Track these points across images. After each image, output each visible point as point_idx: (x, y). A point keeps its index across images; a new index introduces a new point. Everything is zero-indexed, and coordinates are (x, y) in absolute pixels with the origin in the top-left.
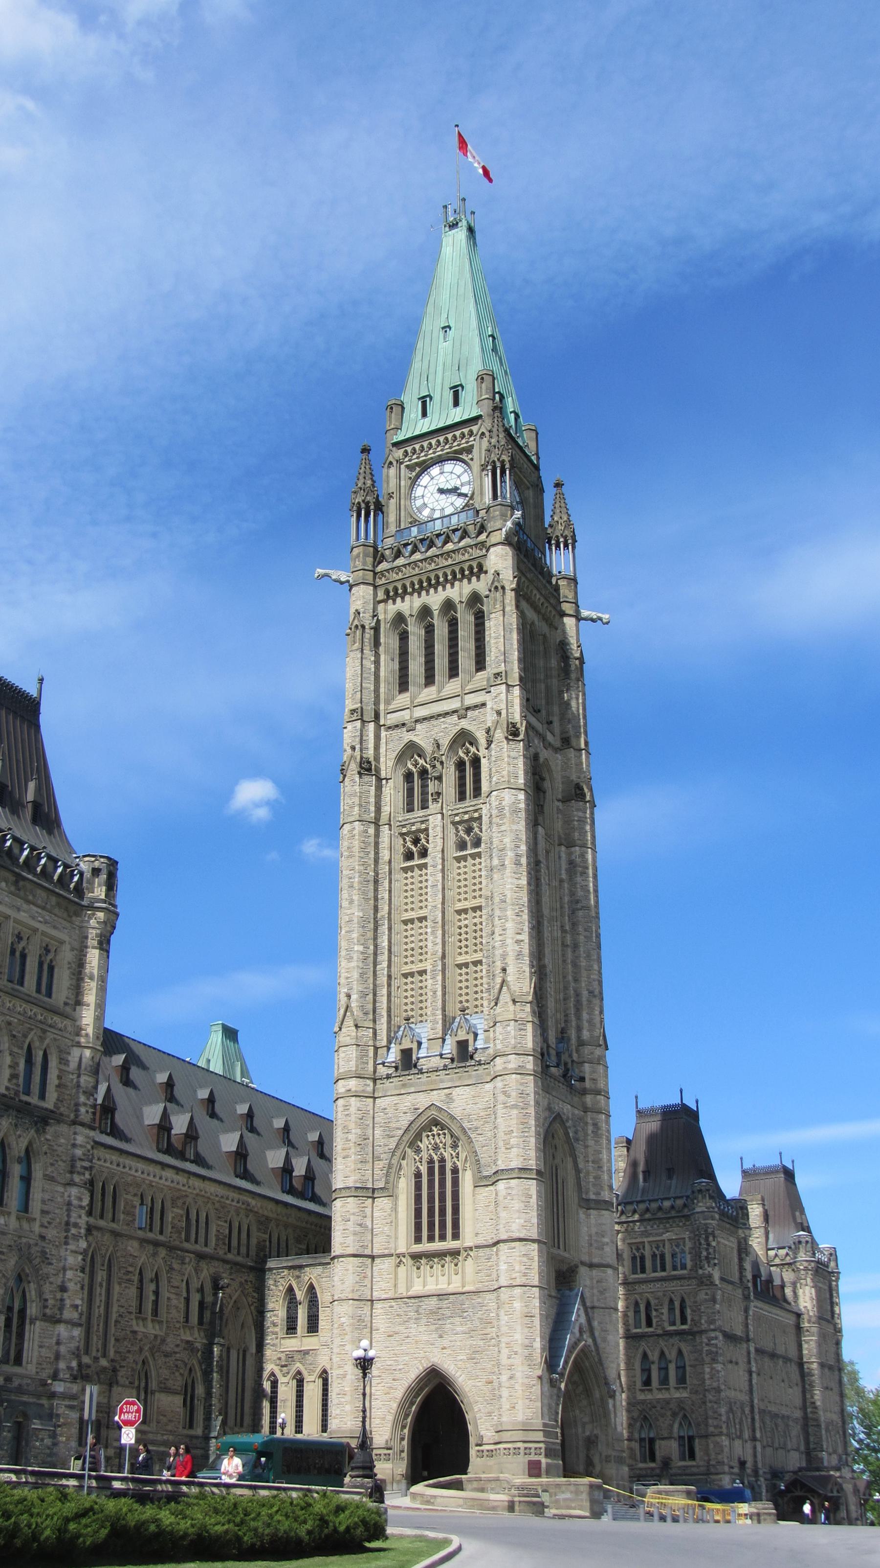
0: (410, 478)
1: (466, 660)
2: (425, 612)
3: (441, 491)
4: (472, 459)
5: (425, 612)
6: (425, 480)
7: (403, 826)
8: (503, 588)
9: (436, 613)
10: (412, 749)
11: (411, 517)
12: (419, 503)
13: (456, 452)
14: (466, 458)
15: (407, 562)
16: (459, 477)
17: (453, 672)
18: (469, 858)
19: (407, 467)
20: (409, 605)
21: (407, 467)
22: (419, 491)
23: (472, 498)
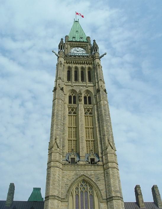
7: (69, 106)
10: (73, 91)
17: (83, 80)
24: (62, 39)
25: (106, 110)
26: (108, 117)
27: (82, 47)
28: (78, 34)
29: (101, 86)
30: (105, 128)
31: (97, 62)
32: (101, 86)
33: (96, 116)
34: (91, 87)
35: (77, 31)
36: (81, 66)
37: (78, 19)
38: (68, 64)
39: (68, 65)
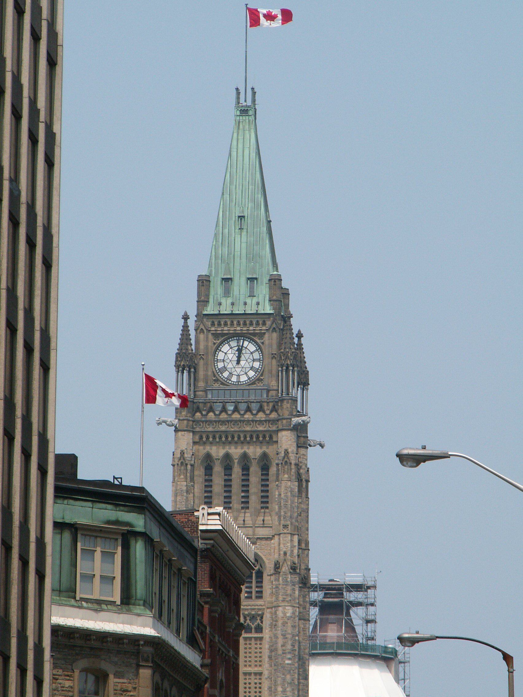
0: (215, 344)
1: (254, 500)
2: (227, 456)
3: (238, 362)
4: (263, 343)
5: (227, 456)
6: (226, 348)
8: (291, 464)
9: (236, 461)
11: (215, 376)
12: (220, 365)
13: (251, 334)
14: (258, 341)
15: (216, 419)
16: (252, 353)
17: (245, 504)
18: (253, 639)
19: (212, 334)
20: (218, 452)
21: (212, 334)
22: (221, 356)
23: (262, 375)
24: (186, 318)
25: (287, 636)
26: (289, 659)
27: (250, 337)
28: (244, 233)
29: (285, 554)
30: (280, 689)
31: (285, 447)
32: (285, 554)
33: (267, 646)
34: (263, 542)
35: (241, 217)
36: (242, 451)
37: (253, 89)
38: (205, 443)
39: (208, 448)
